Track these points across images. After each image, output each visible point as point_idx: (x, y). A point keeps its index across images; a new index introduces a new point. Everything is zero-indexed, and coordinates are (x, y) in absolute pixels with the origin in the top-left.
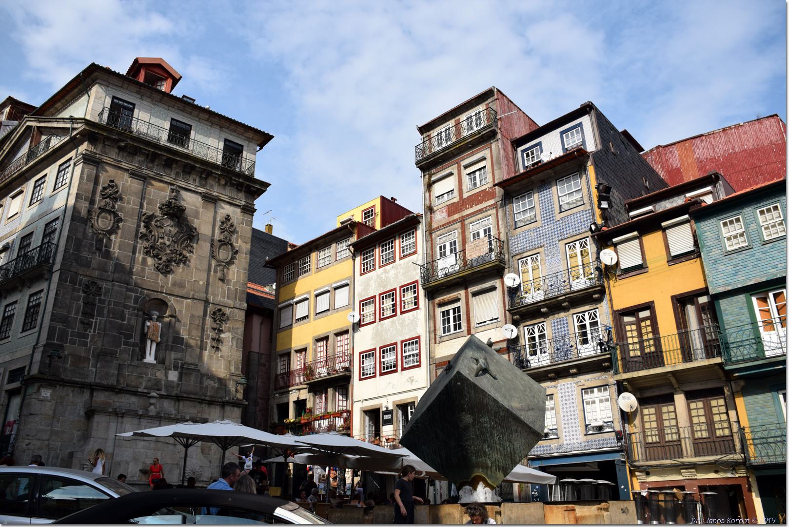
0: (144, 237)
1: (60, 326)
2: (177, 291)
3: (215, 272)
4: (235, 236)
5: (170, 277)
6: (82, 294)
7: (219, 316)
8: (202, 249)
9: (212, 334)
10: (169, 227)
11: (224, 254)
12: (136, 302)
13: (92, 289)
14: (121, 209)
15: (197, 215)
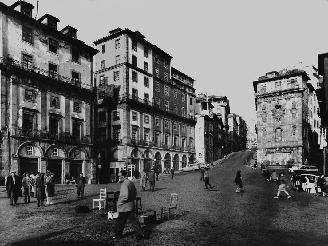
0: (273, 115)
1: (259, 139)
2: (283, 124)
3: (292, 116)
4: (297, 105)
5: (280, 122)
6: (262, 132)
7: (294, 127)
8: (288, 112)
9: (293, 132)
10: (278, 110)
11: (294, 112)
12: (273, 130)
13: (264, 130)
14: (267, 111)
15: (285, 104)
